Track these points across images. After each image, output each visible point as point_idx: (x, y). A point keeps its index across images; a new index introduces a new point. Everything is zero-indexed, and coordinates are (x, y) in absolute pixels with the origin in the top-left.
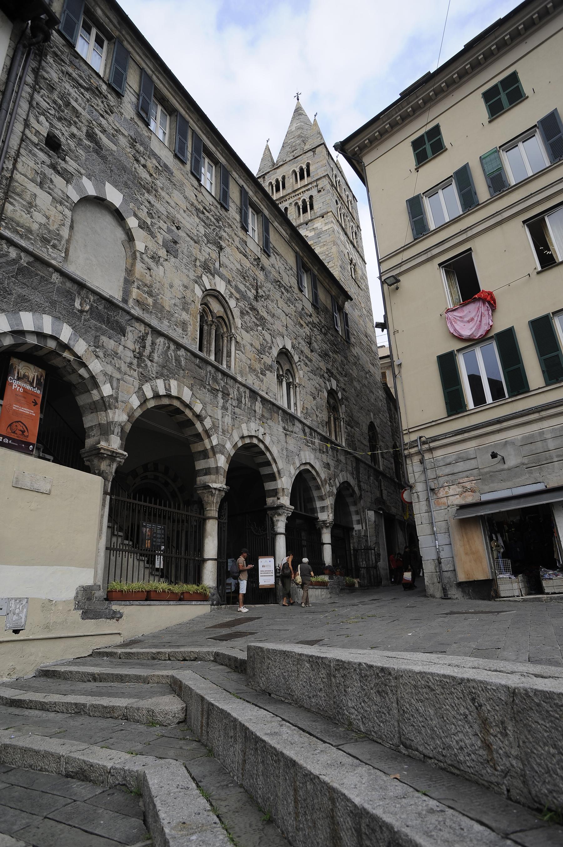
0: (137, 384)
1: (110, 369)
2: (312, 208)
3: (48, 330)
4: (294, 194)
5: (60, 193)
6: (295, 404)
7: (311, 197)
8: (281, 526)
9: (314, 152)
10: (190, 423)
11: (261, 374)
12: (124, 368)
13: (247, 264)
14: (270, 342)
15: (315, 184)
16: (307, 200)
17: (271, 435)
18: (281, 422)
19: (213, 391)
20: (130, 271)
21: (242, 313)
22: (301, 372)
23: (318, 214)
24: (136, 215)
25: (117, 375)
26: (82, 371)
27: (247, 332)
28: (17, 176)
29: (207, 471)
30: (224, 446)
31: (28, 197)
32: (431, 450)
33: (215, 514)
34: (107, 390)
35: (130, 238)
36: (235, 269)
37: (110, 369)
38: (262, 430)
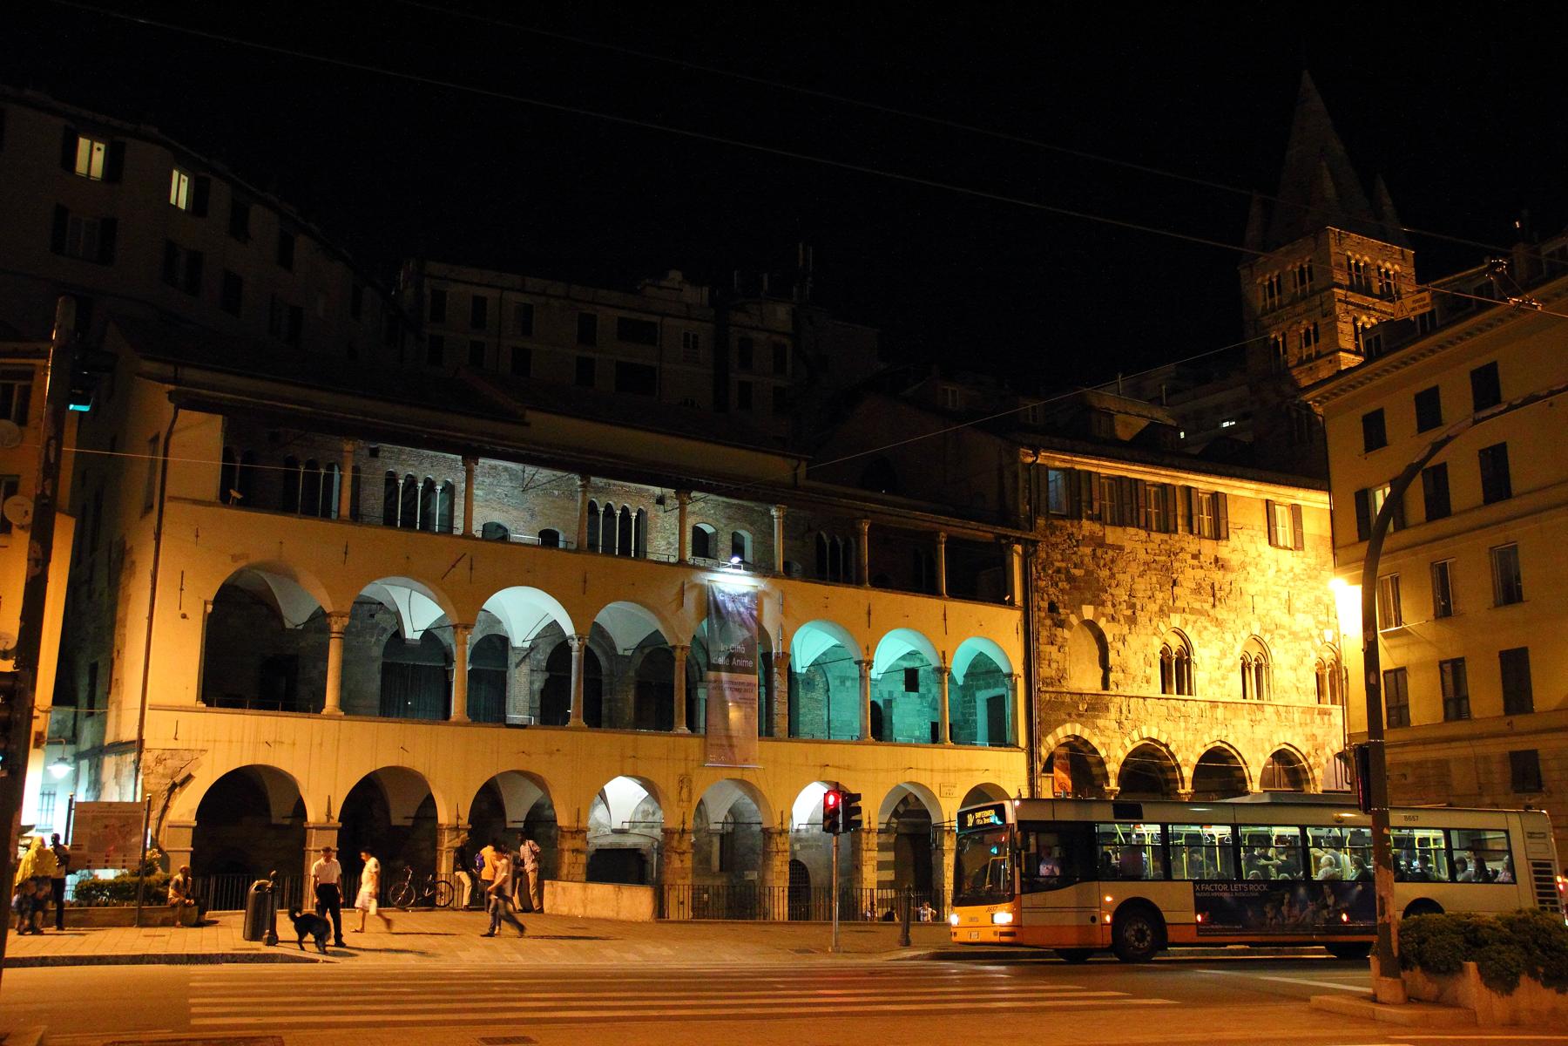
0: (1120, 741)
1: (1103, 740)
2: (1316, 341)
3: (1070, 733)
5: (1060, 640)
7: (1315, 325)
11: (1223, 679)
12: (1111, 734)
15: (1317, 298)
18: (1248, 717)
24: (1103, 615)
25: (1107, 741)
28: (1041, 648)
30: (1188, 760)
31: (1047, 658)
34: (1103, 753)
36: (1188, 592)
37: (1103, 740)
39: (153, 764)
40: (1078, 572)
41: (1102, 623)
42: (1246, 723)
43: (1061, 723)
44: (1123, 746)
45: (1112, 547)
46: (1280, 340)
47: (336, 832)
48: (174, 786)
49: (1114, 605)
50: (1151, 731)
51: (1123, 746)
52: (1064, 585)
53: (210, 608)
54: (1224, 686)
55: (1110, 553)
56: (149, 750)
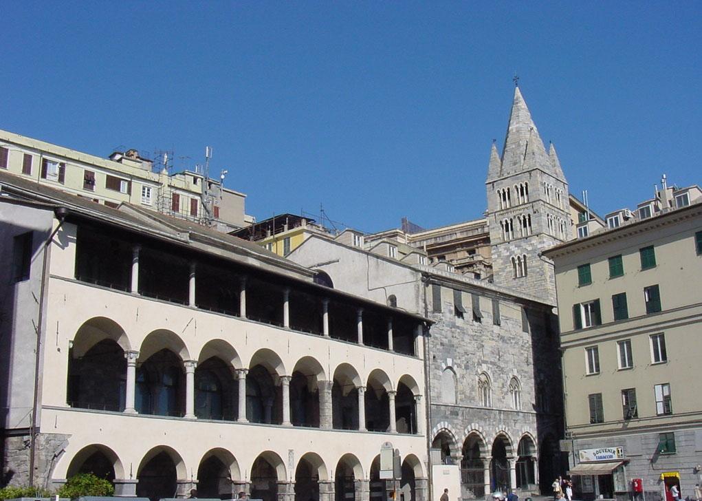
2: (530, 225)
4: (517, 208)
6: (519, 402)
7: (529, 216)
8: (513, 465)
9: (530, 174)
10: (478, 436)
13: (494, 343)
14: (505, 378)
16: (527, 217)
17: (508, 426)
19: (485, 420)
20: (456, 388)
21: (493, 374)
22: (522, 384)
23: (534, 232)
24: (456, 364)
26: (450, 434)
27: (496, 382)
29: (484, 452)
32: (577, 438)
33: (488, 468)
34: (457, 437)
35: (455, 373)
38: (504, 426)
39: (44, 443)
40: (445, 341)
41: (455, 368)
42: (512, 421)
43: (439, 422)
44: (465, 435)
45: (458, 327)
46: (509, 222)
47: (135, 485)
48: (55, 456)
49: (459, 358)
50: (475, 426)
51: (465, 435)
52: (438, 347)
53: (71, 345)
54: (503, 403)
55: (458, 330)
56: (42, 434)
